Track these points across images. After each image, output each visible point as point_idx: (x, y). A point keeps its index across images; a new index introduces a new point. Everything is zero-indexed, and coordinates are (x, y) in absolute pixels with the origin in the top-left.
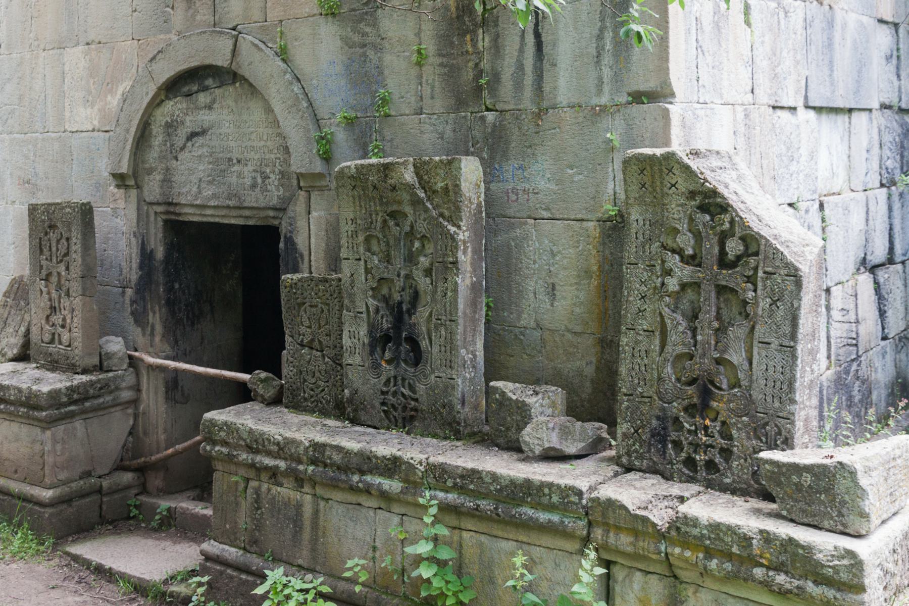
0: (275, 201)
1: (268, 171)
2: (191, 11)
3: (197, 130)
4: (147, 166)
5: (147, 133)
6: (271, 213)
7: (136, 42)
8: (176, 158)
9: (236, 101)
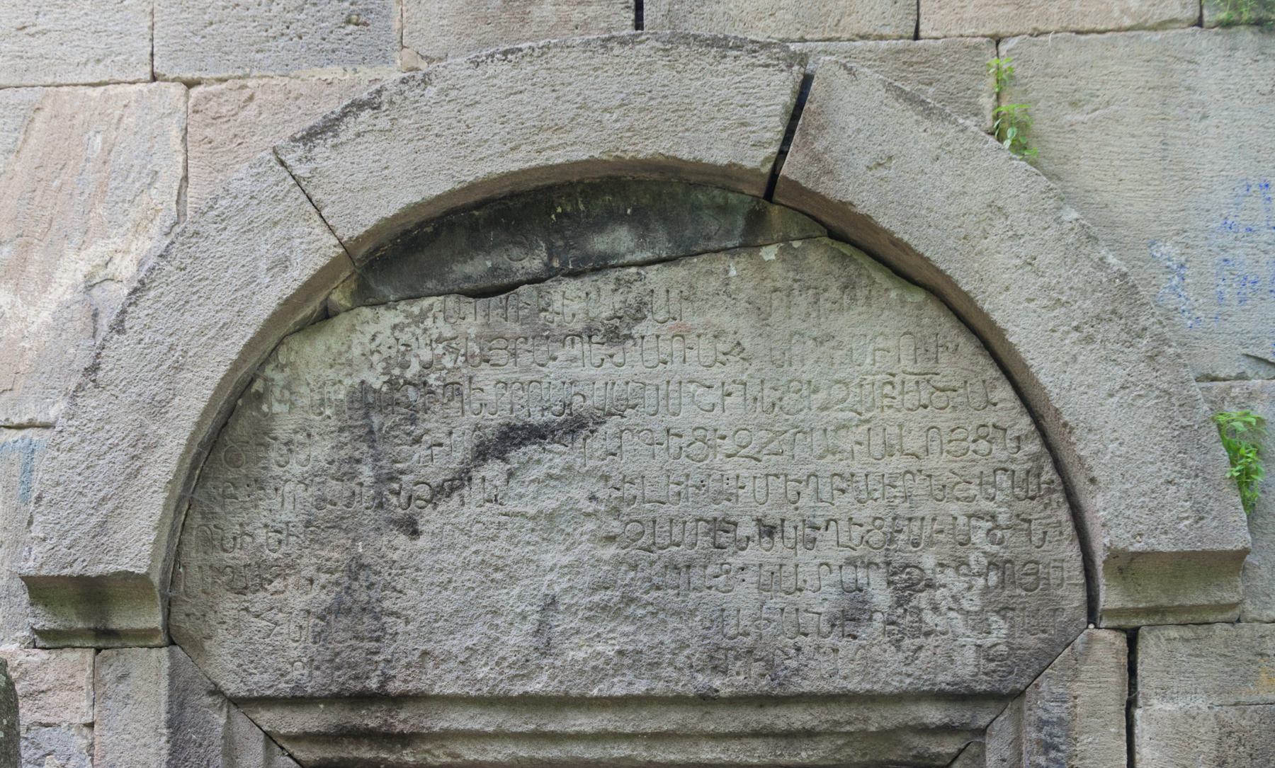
0: (965, 667)
1: (928, 561)
3: (537, 419)
4: (239, 556)
5: (241, 429)
6: (933, 714)
8: (411, 528)
9: (760, 312)
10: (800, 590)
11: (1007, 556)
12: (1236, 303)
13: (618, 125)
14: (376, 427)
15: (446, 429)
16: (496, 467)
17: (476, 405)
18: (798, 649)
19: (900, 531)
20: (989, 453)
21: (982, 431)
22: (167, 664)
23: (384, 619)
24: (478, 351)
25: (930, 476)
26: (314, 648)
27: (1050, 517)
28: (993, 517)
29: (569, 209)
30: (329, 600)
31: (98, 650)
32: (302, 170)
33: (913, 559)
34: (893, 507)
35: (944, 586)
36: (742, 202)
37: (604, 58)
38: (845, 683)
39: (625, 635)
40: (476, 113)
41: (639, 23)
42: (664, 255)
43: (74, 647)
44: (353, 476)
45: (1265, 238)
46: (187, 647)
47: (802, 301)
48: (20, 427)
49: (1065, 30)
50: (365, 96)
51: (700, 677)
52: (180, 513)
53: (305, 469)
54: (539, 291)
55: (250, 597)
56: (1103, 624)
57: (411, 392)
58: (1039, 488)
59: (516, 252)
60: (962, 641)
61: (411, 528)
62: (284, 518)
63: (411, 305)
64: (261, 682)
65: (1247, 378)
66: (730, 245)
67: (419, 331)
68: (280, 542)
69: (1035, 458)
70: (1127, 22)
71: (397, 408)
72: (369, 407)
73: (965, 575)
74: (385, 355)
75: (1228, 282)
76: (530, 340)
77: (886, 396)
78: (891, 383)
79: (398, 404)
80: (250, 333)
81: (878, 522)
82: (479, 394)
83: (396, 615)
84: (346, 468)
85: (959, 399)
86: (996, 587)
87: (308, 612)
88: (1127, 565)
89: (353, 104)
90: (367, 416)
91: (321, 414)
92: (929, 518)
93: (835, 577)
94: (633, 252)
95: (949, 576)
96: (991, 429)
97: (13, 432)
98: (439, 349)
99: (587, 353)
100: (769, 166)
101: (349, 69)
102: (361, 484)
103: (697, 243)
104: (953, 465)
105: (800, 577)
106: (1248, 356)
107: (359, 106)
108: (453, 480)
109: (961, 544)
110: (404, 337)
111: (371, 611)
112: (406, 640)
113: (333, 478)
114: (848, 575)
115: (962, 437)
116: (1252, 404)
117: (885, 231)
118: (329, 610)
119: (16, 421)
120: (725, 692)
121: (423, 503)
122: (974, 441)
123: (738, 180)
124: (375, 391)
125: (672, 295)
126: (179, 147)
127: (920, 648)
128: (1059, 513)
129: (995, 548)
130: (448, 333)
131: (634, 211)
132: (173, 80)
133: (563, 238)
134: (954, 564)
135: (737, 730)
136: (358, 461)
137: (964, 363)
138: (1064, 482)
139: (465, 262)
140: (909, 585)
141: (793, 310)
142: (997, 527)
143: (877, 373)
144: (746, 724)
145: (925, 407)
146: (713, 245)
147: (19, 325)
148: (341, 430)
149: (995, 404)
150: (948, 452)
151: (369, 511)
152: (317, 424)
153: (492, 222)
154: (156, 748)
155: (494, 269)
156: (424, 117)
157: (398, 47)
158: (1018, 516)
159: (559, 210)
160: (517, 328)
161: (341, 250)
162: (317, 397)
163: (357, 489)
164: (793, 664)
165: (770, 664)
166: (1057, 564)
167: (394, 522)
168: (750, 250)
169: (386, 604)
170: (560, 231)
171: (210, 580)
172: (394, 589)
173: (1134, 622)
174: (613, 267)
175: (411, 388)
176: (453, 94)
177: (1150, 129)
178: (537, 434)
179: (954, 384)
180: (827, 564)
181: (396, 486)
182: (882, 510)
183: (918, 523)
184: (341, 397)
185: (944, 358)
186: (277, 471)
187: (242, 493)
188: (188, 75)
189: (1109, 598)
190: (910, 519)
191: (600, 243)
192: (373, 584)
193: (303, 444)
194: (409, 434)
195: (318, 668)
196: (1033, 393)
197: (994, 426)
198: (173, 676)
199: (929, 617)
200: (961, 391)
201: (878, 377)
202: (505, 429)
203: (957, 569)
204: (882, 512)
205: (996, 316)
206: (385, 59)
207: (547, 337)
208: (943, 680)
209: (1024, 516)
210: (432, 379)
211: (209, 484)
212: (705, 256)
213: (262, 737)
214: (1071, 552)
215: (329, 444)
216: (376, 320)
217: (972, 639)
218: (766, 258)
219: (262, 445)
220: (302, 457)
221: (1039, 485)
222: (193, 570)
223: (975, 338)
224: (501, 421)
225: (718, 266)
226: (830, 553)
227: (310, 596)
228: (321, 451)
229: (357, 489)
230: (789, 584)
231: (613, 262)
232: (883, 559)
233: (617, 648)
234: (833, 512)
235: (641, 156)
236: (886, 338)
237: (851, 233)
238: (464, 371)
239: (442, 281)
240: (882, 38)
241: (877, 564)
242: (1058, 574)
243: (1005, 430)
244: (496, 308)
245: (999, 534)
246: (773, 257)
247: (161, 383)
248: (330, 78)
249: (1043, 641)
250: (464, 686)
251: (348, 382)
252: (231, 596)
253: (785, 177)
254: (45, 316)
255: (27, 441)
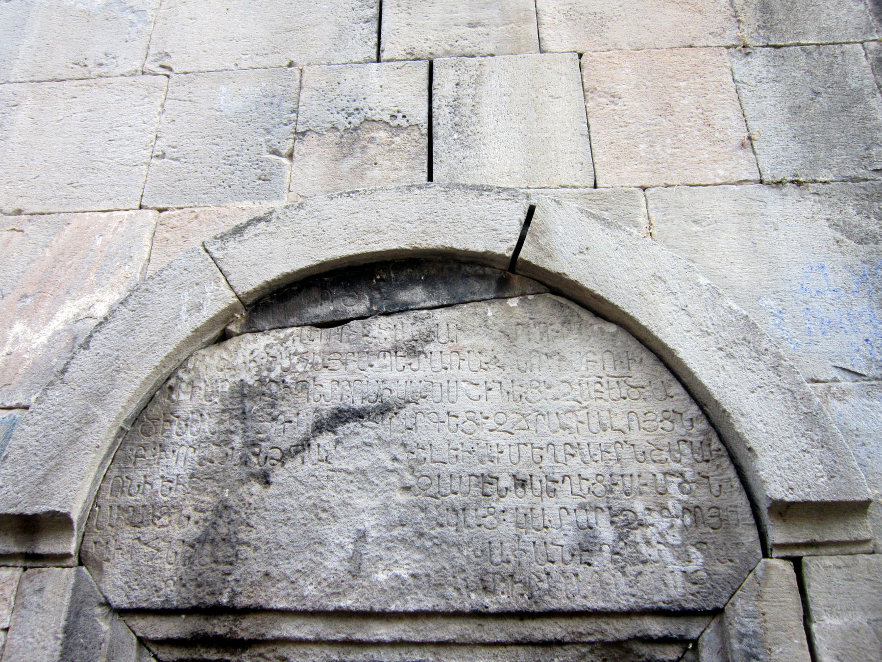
0: (674, 588)
1: (639, 506)
2: (351, 162)
3: (358, 404)
4: (139, 499)
5: (155, 411)
6: (655, 627)
7: (151, 214)
8: (265, 479)
10: (547, 528)
11: (695, 502)
12: (820, 334)
13: (416, 230)
14: (247, 409)
15: (295, 411)
16: (328, 437)
17: (317, 396)
18: (548, 574)
19: (616, 484)
20: (673, 429)
21: (666, 414)
22: (72, 581)
23: (238, 548)
24: (320, 361)
25: (633, 445)
26: (183, 569)
27: (721, 474)
28: (682, 475)
29: (384, 276)
30: (199, 532)
31: (25, 569)
32: (216, 255)
33: (627, 505)
34: (609, 467)
35: (652, 525)
36: (494, 273)
37: (409, 196)
38: (585, 602)
39: (415, 561)
40: (329, 223)
41: (430, 178)
42: (445, 303)
43: (8, 567)
44: (227, 442)
45: (830, 296)
46: (90, 567)
47: (536, 331)
48: (10, 408)
49: (683, 184)
50: (262, 215)
51: (473, 595)
52: (103, 467)
53: (195, 438)
54: (363, 324)
55: (143, 529)
56: (774, 554)
57: (274, 387)
58: (711, 454)
59: (349, 301)
60: (670, 567)
61: (265, 479)
62: (176, 472)
63: (279, 332)
64: (140, 597)
65: (838, 381)
66: (487, 297)
67: (282, 349)
68: (170, 489)
69: (704, 433)
70: (718, 181)
71: (263, 397)
72: (244, 396)
73: (667, 517)
74: (259, 363)
75: (812, 322)
76: (356, 354)
77: (597, 391)
78: (599, 383)
79: (264, 394)
80: (170, 349)
81: (600, 478)
82: (319, 388)
83: (248, 544)
84: (223, 437)
85: (647, 394)
86: (691, 526)
87: (184, 541)
88: (785, 510)
89: (254, 219)
90: (242, 402)
91: (210, 401)
92: (635, 475)
93: (572, 518)
94: (425, 301)
95: (653, 517)
96: (672, 413)
97: (5, 411)
98: (295, 359)
99: (394, 363)
100: (511, 253)
101: (257, 202)
102: (233, 448)
103: (466, 296)
104: (649, 438)
105: (546, 517)
106: (836, 367)
107: (259, 220)
108: (298, 445)
109: (661, 494)
110: (273, 352)
111: (229, 541)
112: (254, 564)
113: (214, 444)
114: (582, 517)
115: (652, 418)
116: (846, 398)
117: (588, 290)
118: (198, 541)
119: (8, 404)
120: (493, 608)
121: (275, 462)
122: (661, 421)
123: (492, 260)
124: (250, 386)
125: (451, 326)
126: (149, 244)
127: (640, 573)
128: (728, 472)
129: (685, 497)
130: (301, 349)
131: (426, 277)
132: (152, 209)
133: (380, 293)
134: (657, 509)
135: (503, 640)
136: (232, 432)
137: (648, 371)
138: (727, 450)
139: (316, 307)
140: (627, 524)
141: (531, 336)
142: (686, 481)
143: (590, 376)
144: (510, 635)
145: (625, 398)
146: (477, 297)
147: (26, 345)
148: (223, 411)
149: (672, 397)
150: (644, 429)
151: (236, 467)
152: (207, 407)
153: (336, 283)
154: (54, 646)
155: (335, 311)
156: (297, 225)
157: (287, 191)
158: (699, 473)
159: (378, 277)
160: (348, 347)
161: (236, 300)
162: (209, 390)
163: (230, 452)
164: (545, 586)
165: (527, 585)
166: (732, 509)
167: (252, 475)
168: (501, 300)
169: (241, 536)
170: (378, 289)
171: (116, 516)
172: (248, 525)
173: (797, 553)
174: (412, 310)
175: (273, 384)
176: (316, 213)
177: (744, 236)
178: (358, 415)
179: (642, 383)
180: (565, 508)
181: (257, 450)
182: (601, 469)
183: (628, 478)
184: (226, 390)
185: (634, 367)
186: (176, 438)
187: (148, 454)
188: (161, 206)
189: (777, 535)
190: (622, 476)
191: (404, 296)
192: (232, 521)
193: (196, 421)
194: (269, 414)
195: (184, 585)
196: (697, 390)
197: (673, 411)
198: (75, 589)
199: (643, 548)
200: (648, 388)
201: (590, 379)
202: (336, 411)
203: (660, 512)
204: (602, 470)
205: (666, 341)
206: (279, 197)
207: (368, 353)
208: (659, 599)
209: (704, 474)
210: (288, 379)
211: (128, 447)
212: (472, 304)
213: (135, 640)
214: (741, 500)
215: (214, 420)
216: (255, 341)
217: (678, 567)
218: (511, 305)
219: (168, 421)
220: (195, 429)
221: (710, 452)
222: (106, 510)
223: (652, 355)
224: (333, 406)
225: (480, 310)
226: (566, 500)
227: (186, 529)
228: (208, 425)
229: (230, 452)
230: (539, 522)
231: (412, 307)
232: (605, 504)
233: (411, 572)
234: (566, 470)
235: (430, 247)
236: (594, 354)
237: (565, 290)
238: (310, 373)
239: (301, 318)
240: (575, 187)
241: (601, 508)
242: (734, 516)
243: (681, 414)
244: (335, 334)
245: (687, 486)
246: (516, 305)
247: (105, 381)
248: (244, 207)
249: (731, 568)
250: (293, 601)
251: (232, 380)
252: (129, 528)
253: (521, 259)
254: (44, 339)
255: (12, 417)
